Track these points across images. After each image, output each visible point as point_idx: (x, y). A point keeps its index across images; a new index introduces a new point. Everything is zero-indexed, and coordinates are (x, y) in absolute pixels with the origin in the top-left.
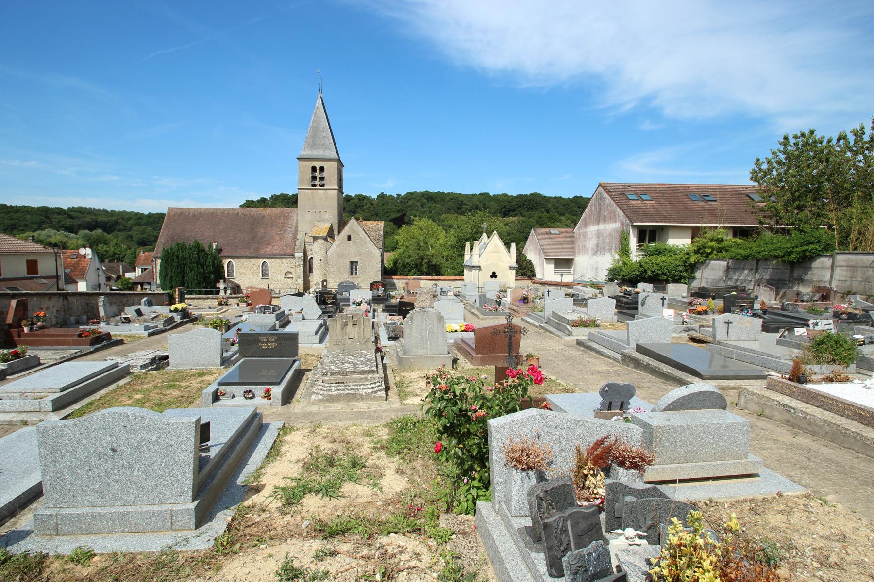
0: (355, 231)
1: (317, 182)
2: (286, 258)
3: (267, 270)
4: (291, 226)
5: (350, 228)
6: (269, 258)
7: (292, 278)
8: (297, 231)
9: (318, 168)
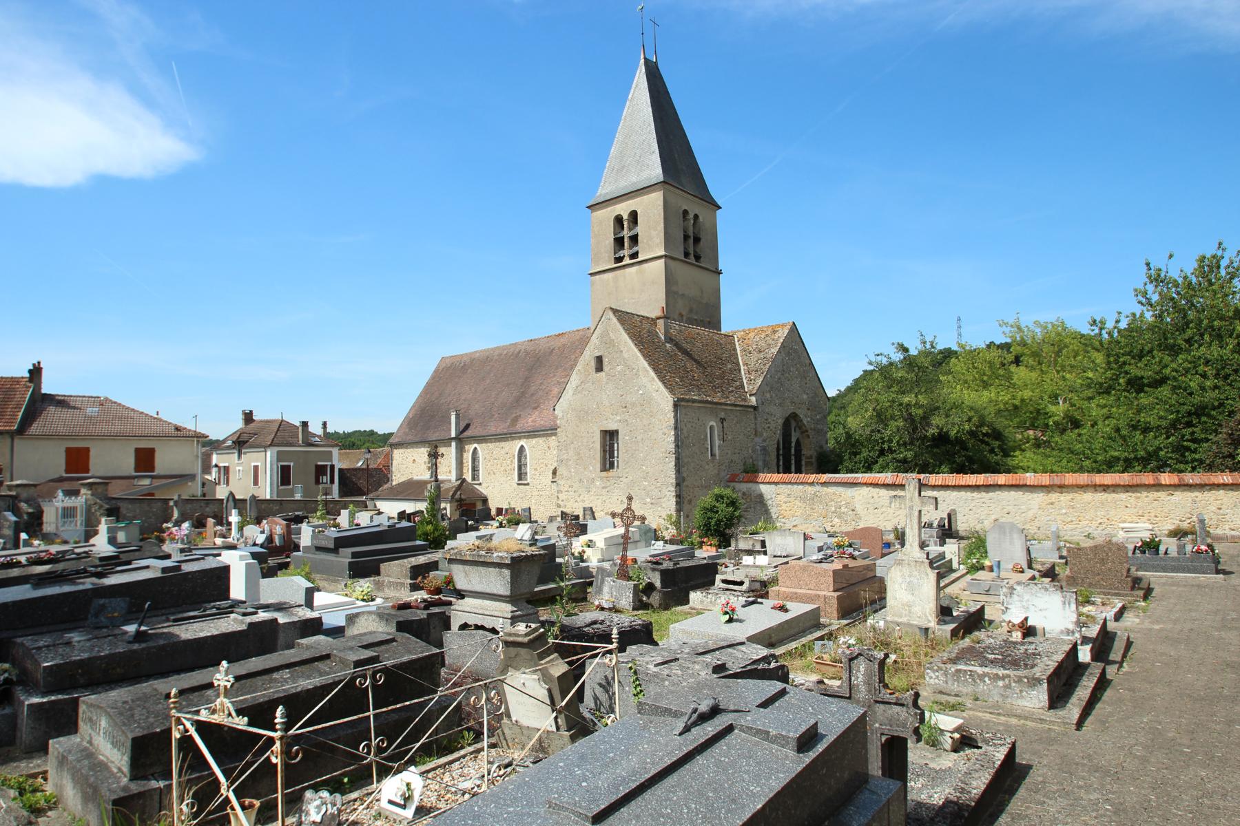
1: (626, 252)
5: (602, 336)
6: (528, 437)
9: (625, 217)
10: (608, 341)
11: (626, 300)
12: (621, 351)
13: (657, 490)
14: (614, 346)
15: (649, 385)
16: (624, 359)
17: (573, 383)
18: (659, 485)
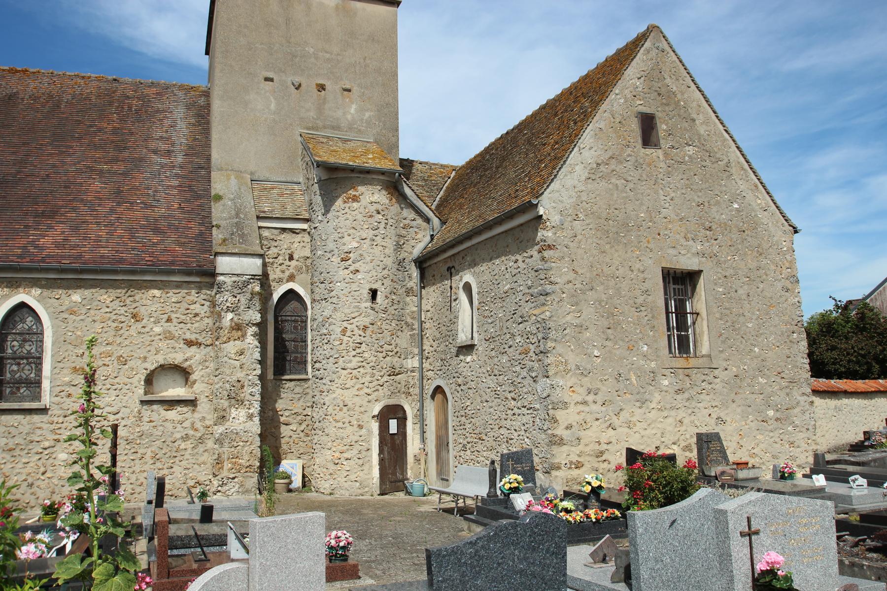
0: (666, 97)
3: (38, 361)
4: (163, 146)
7: (192, 403)
8: (207, 166)
10: (663, 91)
12: (694, 120)
13: (782, 394)
14: (677, 103)
15: (750, 196)
16: (699, 136)
17: (586, 154)
18: (784, 384)
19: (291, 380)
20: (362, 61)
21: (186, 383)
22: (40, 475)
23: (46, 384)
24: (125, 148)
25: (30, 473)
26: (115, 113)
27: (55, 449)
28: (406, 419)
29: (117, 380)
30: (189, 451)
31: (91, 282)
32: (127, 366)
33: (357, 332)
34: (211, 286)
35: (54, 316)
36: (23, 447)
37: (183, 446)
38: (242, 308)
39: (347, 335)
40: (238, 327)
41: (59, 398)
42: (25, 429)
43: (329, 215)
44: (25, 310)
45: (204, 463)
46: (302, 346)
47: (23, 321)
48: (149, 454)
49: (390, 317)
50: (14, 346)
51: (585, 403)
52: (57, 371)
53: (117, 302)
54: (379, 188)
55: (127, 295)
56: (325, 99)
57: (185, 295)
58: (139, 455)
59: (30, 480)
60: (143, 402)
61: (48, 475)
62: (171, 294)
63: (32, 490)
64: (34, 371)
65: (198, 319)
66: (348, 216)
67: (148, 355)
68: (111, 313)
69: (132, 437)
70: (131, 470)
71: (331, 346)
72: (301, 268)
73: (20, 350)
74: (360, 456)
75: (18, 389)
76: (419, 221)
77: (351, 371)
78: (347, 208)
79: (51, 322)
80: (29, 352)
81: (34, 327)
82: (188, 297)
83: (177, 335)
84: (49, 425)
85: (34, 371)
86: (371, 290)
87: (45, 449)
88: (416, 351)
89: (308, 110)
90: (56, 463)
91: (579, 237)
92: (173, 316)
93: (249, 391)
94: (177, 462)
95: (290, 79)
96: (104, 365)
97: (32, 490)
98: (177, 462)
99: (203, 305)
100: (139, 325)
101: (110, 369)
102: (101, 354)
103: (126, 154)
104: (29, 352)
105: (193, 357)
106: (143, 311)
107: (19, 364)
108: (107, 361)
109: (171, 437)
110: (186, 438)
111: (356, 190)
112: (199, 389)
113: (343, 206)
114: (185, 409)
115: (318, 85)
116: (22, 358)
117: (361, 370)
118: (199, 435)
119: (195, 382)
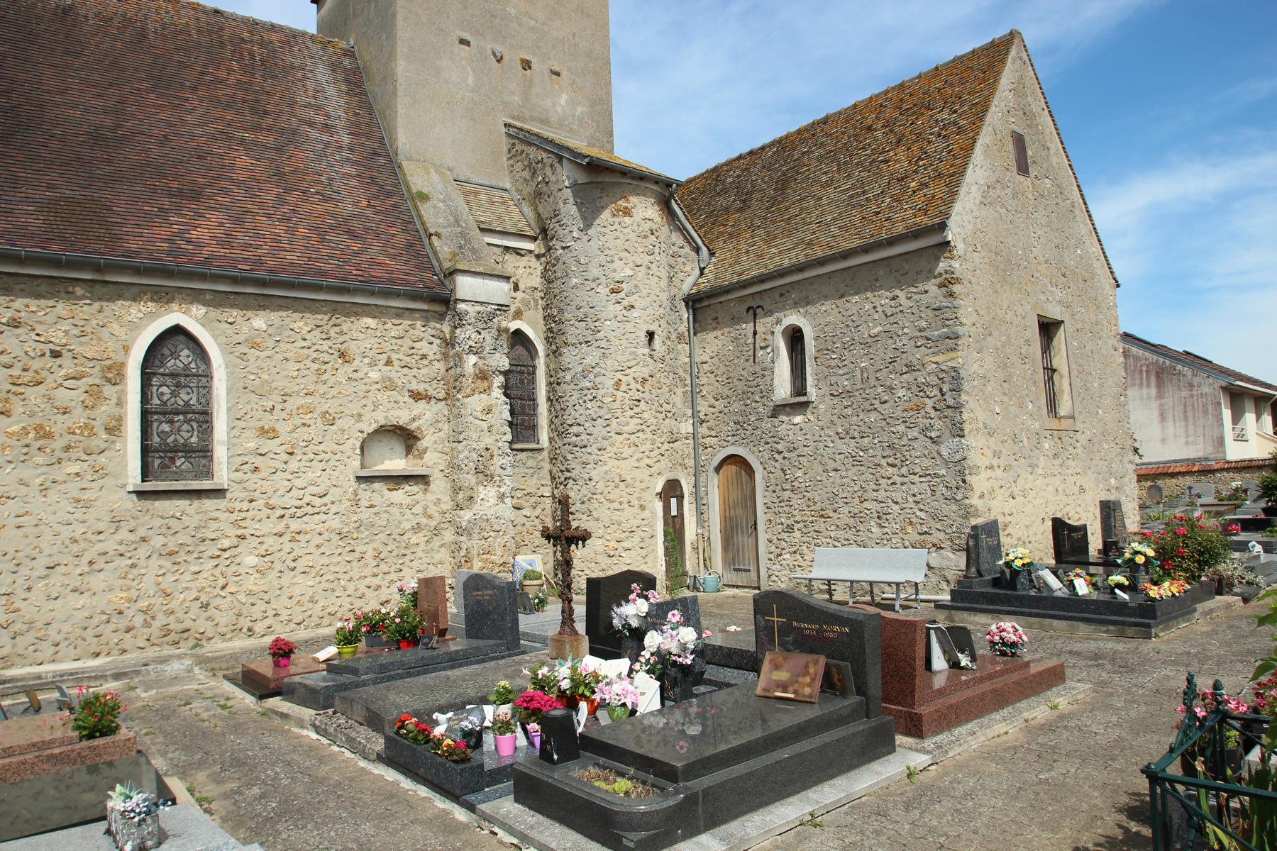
2: (377, 312)
3: (204, 418)
6: (218, 301)
7: (423, 479)
11: (514, 12)
19: (522, 450)
20: (571, 37)
21: (407, 455)
22: (217, 591)
23: (220, 453)
24: (265, 112)
25: (204, 588)
26: (232, 60)
27: (239, 550)
28: (683, 497)
29: (322, 447)
30: (422, 547)
31: (280, 302)
32: (334, 427)
33: (634, 385)
34: (441, 317)
35: (229, 347)
36: (191, 549)
37: (414, 541)
38: (487, 349)
39: (621, 389)
40: (483, 375)
41: (241, 472)
42: (194, 521)
43: (592, 232)
44: (181, 338)
45: (441, 563)
46: (529, 405)
47: (175, 355)
48: (370, 553)
49: (667, 369)
50: (162, 394)
51: (991, 468)
52: (236, 432)
53: (317, 332)
54: (653, 201)
55: (331, 323)
56: (531, 81)
57: (408, 328)
58: (357, 555)
59: (204, 599)
60: (359, 479)
61: (230, 589)
62: (389, 326)
63: (209, 613)
64: (196, 433)
65: (425, 362)
66: (618, 233)
67: (363, 412)
68: (309, 348)
69: (346, 529)
70: (347, 577)
71: (599, 404)
72: (529, 302)
73: (173, 400)
74: (642, 545)
75: (173, 460)
76: (687, 249)
77: (628, 436)
78: (616, 224)
79: (224, 359)
80: (187, 403)
81: (193, 365)
82: (412, 331)
83: (400, 384)
84: (229, 514)
85: (196, 433)
86: (647, 332)
87: (225, 550)
88: (689, 412)
89: (513, 93)
90: (242, 570)
91: (978, 271)
92: (394, 357)
93: (500, 463)
94: (408, 562)
95: (489, 46)
96: (304, 424)
97: (209, 613)
98: (408, 562)
99: (431, 343)
100: (348, 369)
101: (312, 430)
102: (298, 409)
103: (269, 121)
104: (187, 403)
105: (423, 416)
106: (353, 348)
107: (171, 422)
108: (307, 418)
109: (398, 527)
110: (417, 528)
111: (627, 201)
112: (431, 460)
113: (611, 220)
114: (415, 489)
115: (523, 61)
116: (177, 413)
117: (640, 434)
118: (434, 523)
119: (425, 451)
